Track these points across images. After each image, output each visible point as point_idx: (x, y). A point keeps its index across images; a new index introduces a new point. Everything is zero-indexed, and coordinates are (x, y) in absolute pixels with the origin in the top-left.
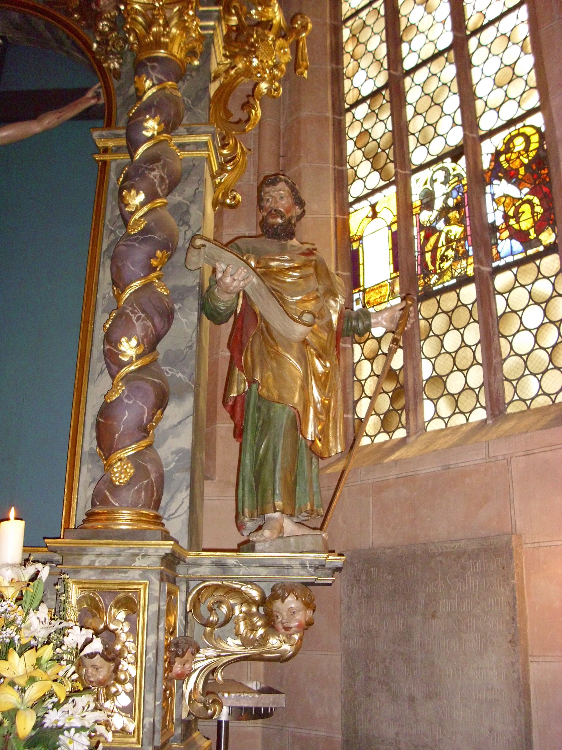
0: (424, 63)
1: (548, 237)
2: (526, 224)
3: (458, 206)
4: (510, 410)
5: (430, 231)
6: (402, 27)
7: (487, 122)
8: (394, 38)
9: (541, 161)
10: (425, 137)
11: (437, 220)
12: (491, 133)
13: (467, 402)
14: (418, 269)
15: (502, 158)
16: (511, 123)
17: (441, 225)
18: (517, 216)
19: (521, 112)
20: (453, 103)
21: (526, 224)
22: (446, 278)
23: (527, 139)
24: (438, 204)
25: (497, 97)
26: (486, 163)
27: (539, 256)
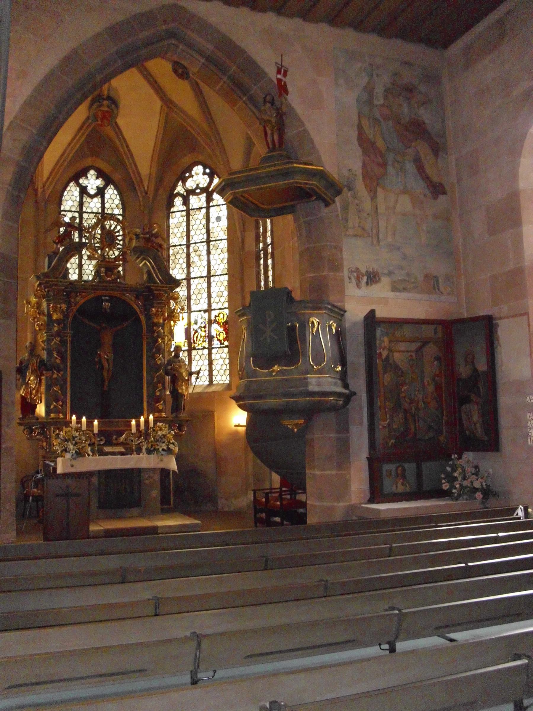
0: (197, 278)
1: (226, 343)
2: (221, 338)
3: (205, 327)
4: (214, 383)
5: (196, 331)
6: (191, 261)
7: (214, 306)
8: (189, 266)
9: (226, 323)
10: (196, 302)
11: (198, 329)
12: (215, 310)
13: (203, 379)
14: (192, 341)
15: (217, 318)
16: (220, 309)
17: (199, 331)
18: (219, 335)
19: (223, 307)
20: (205, 295)
21: (221, 338)
22: (200, 345)
23: (224, 315)
24: (199, 324)
25: (217, 300)
26: (213, 318)
27: (223, 347)
